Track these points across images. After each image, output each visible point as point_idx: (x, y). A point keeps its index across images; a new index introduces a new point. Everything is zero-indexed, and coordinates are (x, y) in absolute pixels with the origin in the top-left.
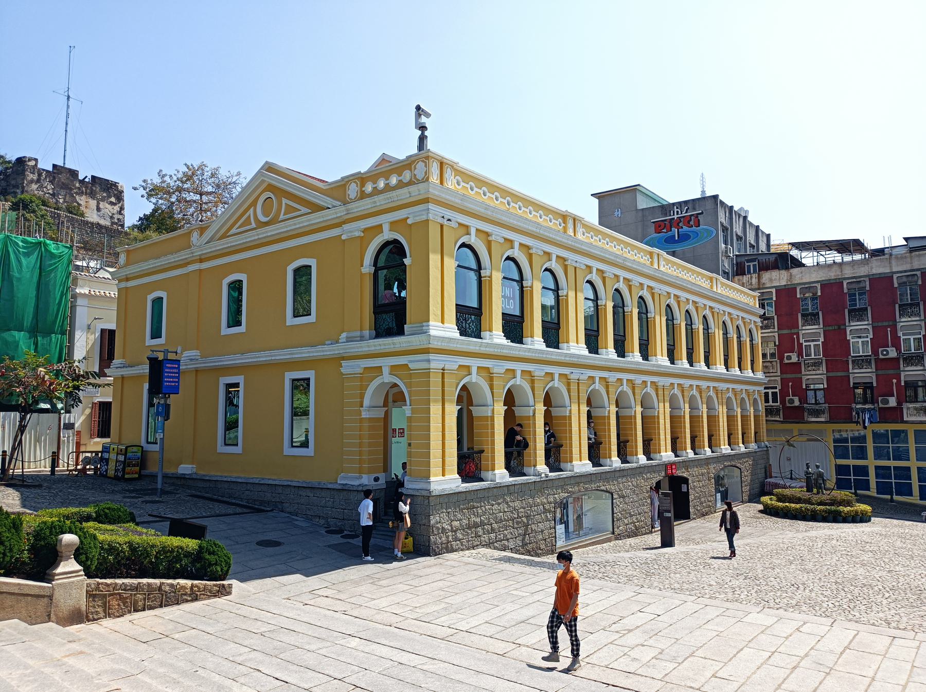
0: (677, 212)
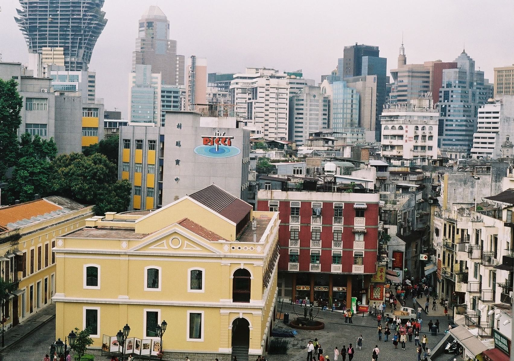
0: (218, 134)
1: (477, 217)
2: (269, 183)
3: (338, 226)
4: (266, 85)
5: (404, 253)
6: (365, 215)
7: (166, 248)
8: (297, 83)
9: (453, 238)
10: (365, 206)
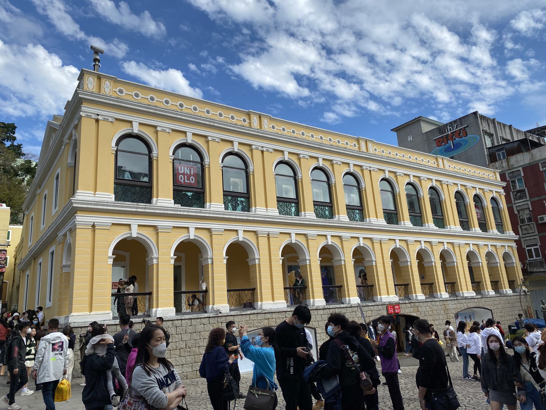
0: (450, 129)
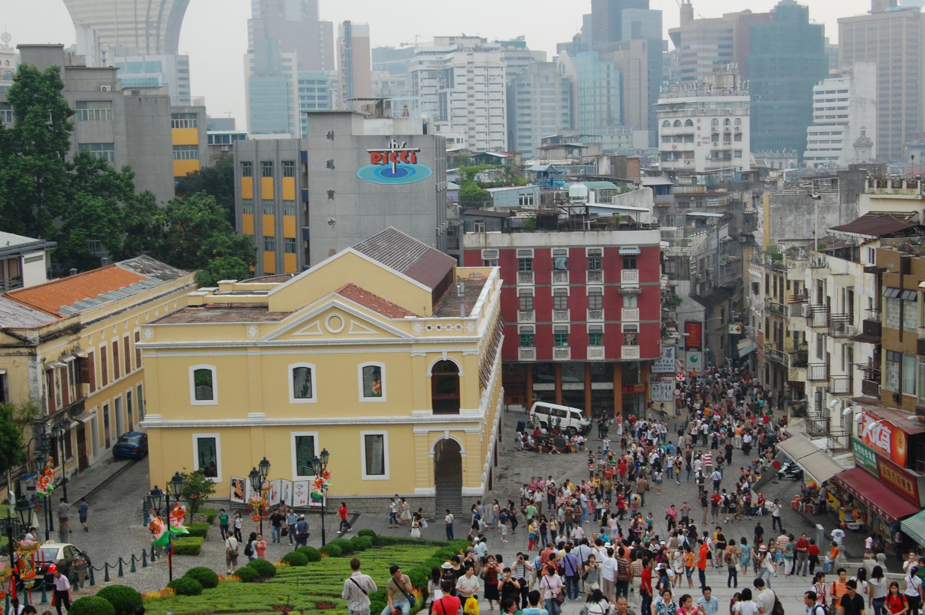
1: (819, 260)
2: (482, 221)
3: (595, 285)
4: (469, 63)
5: (703, 325)
6: (638, 265)
7: (321, 333)
8: (519, 58)
9: (782, 295)
10: (637, 252)
